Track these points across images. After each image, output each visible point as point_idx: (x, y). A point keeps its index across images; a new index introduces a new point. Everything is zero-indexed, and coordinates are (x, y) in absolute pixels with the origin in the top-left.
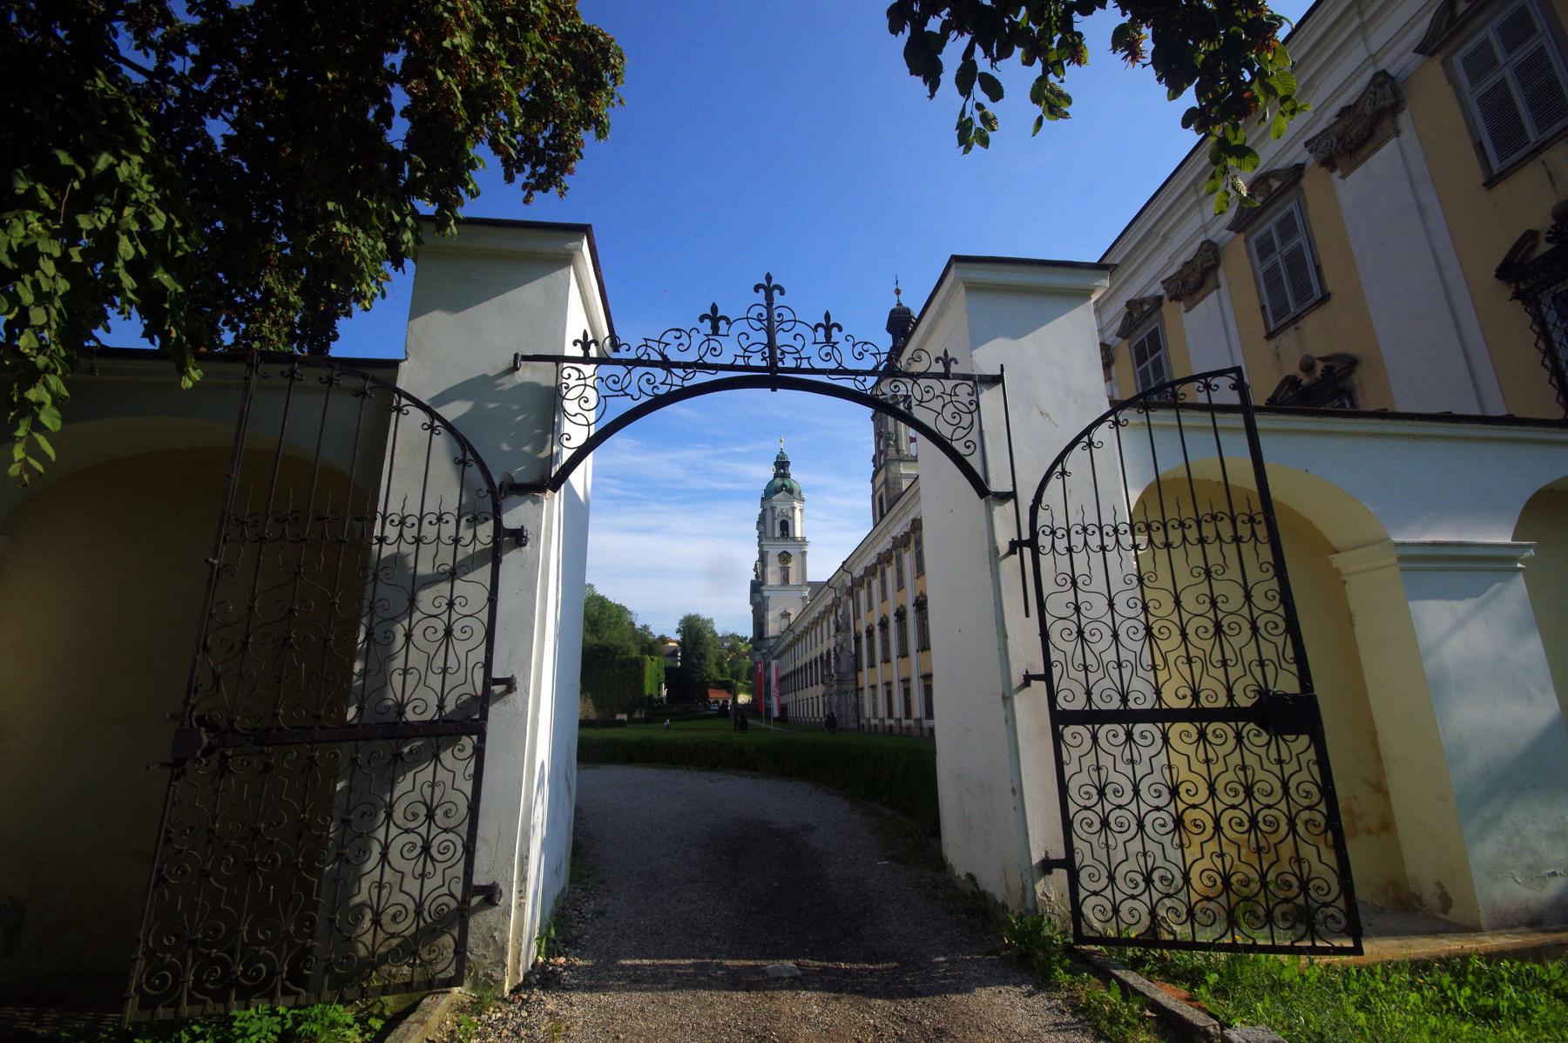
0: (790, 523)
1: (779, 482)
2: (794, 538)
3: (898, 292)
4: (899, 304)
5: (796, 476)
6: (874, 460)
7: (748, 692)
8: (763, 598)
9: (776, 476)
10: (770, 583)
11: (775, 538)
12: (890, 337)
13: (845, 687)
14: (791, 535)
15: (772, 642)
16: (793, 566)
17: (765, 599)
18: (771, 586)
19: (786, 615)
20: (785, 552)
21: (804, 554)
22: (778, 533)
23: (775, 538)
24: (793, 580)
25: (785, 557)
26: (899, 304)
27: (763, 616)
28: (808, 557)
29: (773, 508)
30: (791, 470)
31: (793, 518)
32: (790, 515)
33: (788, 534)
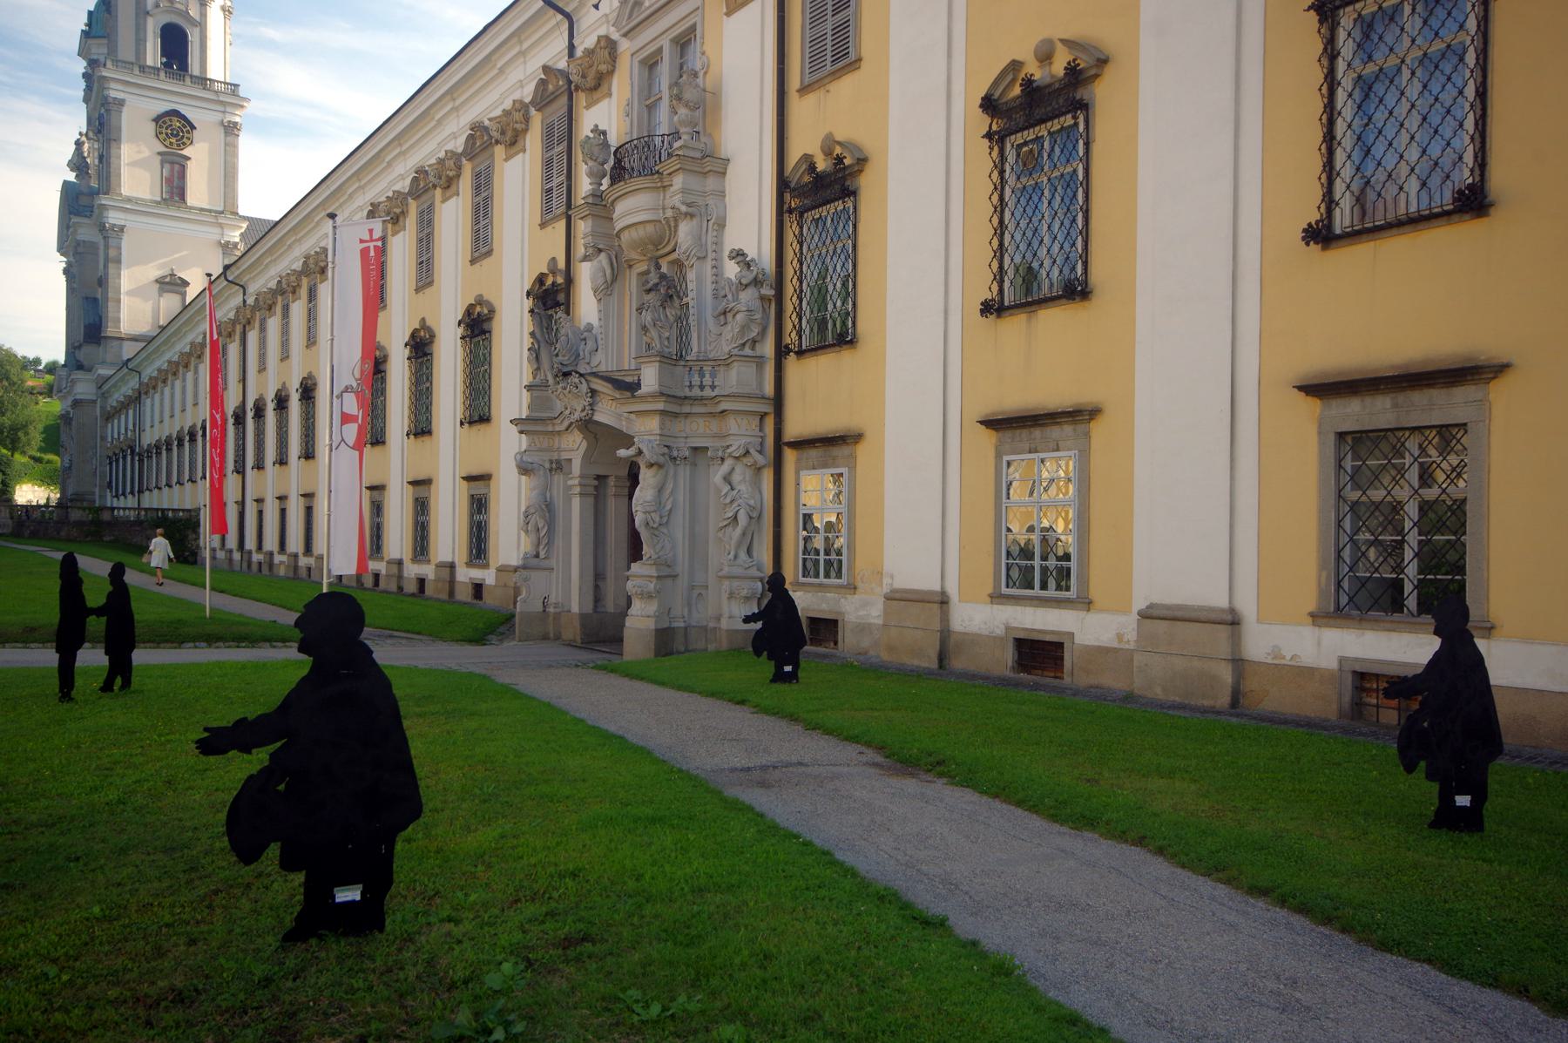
0: (193, 36)
2: (203, 81)
7: (45, 479)
8: (102, 228)
10: (126, 190)
11: (143, 68)
13: (697, 431)
14: (194, 68)
15: (129, 350)
16: (199, 155)
17: (108, 235)
18: (129, 200)
19: (172, 284)
20: (175, 113)
21: (231, 129)
23: (143, 68)
24: (199, 191)
27: (102, 282)
28: (245, 142)
31: (202, 25)
32: (194, 12)
33: (184, 66)
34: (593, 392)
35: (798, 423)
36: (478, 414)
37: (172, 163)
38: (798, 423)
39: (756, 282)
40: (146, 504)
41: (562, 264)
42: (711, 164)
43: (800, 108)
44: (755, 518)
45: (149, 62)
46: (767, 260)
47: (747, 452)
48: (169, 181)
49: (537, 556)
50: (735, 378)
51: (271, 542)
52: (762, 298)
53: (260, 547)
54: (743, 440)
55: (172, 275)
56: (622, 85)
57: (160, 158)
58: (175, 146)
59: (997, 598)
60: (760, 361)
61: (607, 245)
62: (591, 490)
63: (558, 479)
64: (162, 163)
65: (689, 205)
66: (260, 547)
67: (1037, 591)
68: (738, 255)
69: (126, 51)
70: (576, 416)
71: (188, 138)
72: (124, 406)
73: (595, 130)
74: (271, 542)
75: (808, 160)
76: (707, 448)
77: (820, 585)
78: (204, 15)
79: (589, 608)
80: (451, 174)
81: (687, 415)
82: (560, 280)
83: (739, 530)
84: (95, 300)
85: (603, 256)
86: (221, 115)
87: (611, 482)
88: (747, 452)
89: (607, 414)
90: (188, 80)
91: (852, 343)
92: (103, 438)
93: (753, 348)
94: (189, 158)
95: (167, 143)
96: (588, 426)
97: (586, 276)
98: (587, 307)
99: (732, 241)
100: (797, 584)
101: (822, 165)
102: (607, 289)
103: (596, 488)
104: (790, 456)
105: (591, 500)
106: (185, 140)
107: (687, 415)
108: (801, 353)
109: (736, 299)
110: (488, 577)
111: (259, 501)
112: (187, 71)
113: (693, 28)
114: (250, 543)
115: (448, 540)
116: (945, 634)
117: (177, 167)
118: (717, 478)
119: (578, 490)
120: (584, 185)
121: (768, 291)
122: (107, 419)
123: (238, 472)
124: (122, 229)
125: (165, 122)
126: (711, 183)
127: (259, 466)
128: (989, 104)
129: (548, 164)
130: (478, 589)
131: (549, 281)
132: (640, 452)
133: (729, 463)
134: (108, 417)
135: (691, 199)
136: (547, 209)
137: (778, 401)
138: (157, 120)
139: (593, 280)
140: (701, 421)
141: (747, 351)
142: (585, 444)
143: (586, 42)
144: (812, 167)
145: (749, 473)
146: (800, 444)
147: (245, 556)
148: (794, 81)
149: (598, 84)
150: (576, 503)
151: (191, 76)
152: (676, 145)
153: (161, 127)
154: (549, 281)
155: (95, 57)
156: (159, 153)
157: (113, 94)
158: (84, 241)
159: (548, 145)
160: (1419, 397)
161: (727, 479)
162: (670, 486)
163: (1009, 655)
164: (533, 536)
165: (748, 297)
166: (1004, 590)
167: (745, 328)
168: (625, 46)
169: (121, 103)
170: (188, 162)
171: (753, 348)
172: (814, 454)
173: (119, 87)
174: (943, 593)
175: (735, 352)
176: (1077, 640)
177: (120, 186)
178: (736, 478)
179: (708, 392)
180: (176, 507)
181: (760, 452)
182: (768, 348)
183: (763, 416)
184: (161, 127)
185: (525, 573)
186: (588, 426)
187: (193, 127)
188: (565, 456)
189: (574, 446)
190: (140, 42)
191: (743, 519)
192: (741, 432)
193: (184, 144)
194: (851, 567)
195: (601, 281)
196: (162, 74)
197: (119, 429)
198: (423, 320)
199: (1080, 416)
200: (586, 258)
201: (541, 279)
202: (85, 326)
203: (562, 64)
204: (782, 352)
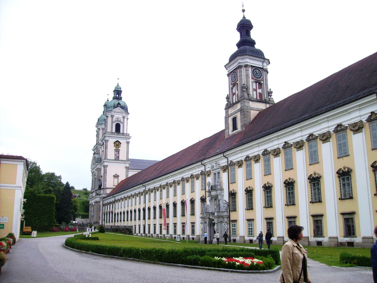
1: (116, 102)
3: (244, 11)
4: (244, 17)
5: (125, 98)
6: (228, 98)
9: (114, 98)
11: (112, 133)
12: (238, 34)
14: (121, 132)
21: (128, 143)
22: (114, 131)
24: (122, 156)
25: (117, 144)
26: (244, 17)
29: (112, 116)
30: (122, 95)
31: (123, 123)
32: (122, 121)
34: (210, 215)
35: (232, 218)
36: (193, 214)
37: (116, 151)
38: (232, 218)
39: (227, 203)
40: (117, 224)
41: (204, 196)
42: (222, 189)
43: (230, 185)
44: (228, 229)
45: (113, 132)
46: (228, 201)
47: (226, 222)
48: (115, 155)
49: (203, 233)
50: (226, 214)
51: (152, 232)
52: (228, 205)
53: (149, 233)
54: (226, 220)
55: (116, 174)
56: (212, 175)
57: (114, 150)
58: (117, 148)
59: (248, 236)
60: (228, 212)
61: (210, 195)
62: (209, 225)
63: (205, 224)
64: (115, 151)
65: (219, 194)
66: (149, 233)
67: (251, 235)
68: (225, 200)
69: (109, 130)
70: (208, 217)
71: (120, 146)
72: (110, 203)
73: (209, 182)
74: (152, 232)
75: (231, 191)
76: (222, 221)
77: (234, 236)
78: (124, 121)
79: (210, 240)
80: (188, 180)
81: (220, 218)
82: (204, 198)
83: (226, 230)
84: (100, 180)
85: (210, 197)
86: (126, 140)
87: (212, 224)
88: (226, 222)
89: (211, 217)
90: (120, 134)
91: (236, 211)
92: (103, 210)
93: (227, 210)
94: (120, 150)
95: (116, 147)
96: (209, 218)
97: (208, 199)
98: (208, 202)
99: (224, 199)
100: (232, 236)
101: (232, 192)
102: (210, 201)
103: (210, 225)
104: (231, 222)
105: (209, 227)
106: (119, 146)
107: (220, 218)
108: (231, 211)
109: (225, 205)
110: (194, 237)
111: (149, 225)
112: (120, 132)
113: (220, 172)
114: (147, 232)
115: (188, 231)
116: (244, 240)
117: (117, 152)
118: (223, 224)
119: (208, 225)
120: (207, 189)
121: (228, 204)
122: (104, 206)
123: (144, 219)
124: (107, 166)
125: (116, 143)
126: (222, 191)
127: (149, 218)
128: (245, 191)
129: (202, 182)
130: (193, 238)
131: (203, 198)
132: (215, 222)
133: (224, 223)
134: (104, 205)
135: (219, 193)
136: (202, 188)
137: (229, 216)
138: (114, 143)
139: (209, 200)
140: (221, 218)
141: (226, 211)
142: (208, 220)
143: (207, 170)
144: (231, 192)
145: (227, 224)
146: (232, 221)
147: (146, 235)
148: (230, 183)
149: (209, 175)
150: (208, 227)
151: (121, 133)
152: (218, 187)
153: (115, 144)
154: (203, 198)
155: (99, 128)
156: (115, 150)
157: (107, 139)
158: (99, 168)
159: (202, 180)
160: (270, 220)
161: (224, 224)
162: (218, 225)
163: (249, 241)
164: (202, 231)
165: (226, 205)
166: (249, 235)
167: (226, 208)
168: (211, 171)
169: (108, 140)
170: (120, 151)
171: (227, 210)
172: (233, 222)
173: (108, 137)
174: (244, 236)
175: (225, 211)
176: (254, 240)
177: (107, 157)
178: (225, 224)
179: (222, 215)
180: (129, 226)
181: (228, 222)
182: (228, 210)
183: (228, 218)
184: (115, 144)
185: (202, 236)
186: (209, 218)
187: (121, 143)
188: (206, 221)
189: (207, 220)
190: (112, 128)
191: (226, 229)
192: (226, 220)
193: (119, 147)
194: (237, 234)
195: (210, 200)
196: (116, 133)
197: (108, 209)
198: (183, 199)
199: (253, 220)
200: (208, 197)
201: (202, 197)
202: (99, 186)
203: (204, 171)
204: (230, 211)
